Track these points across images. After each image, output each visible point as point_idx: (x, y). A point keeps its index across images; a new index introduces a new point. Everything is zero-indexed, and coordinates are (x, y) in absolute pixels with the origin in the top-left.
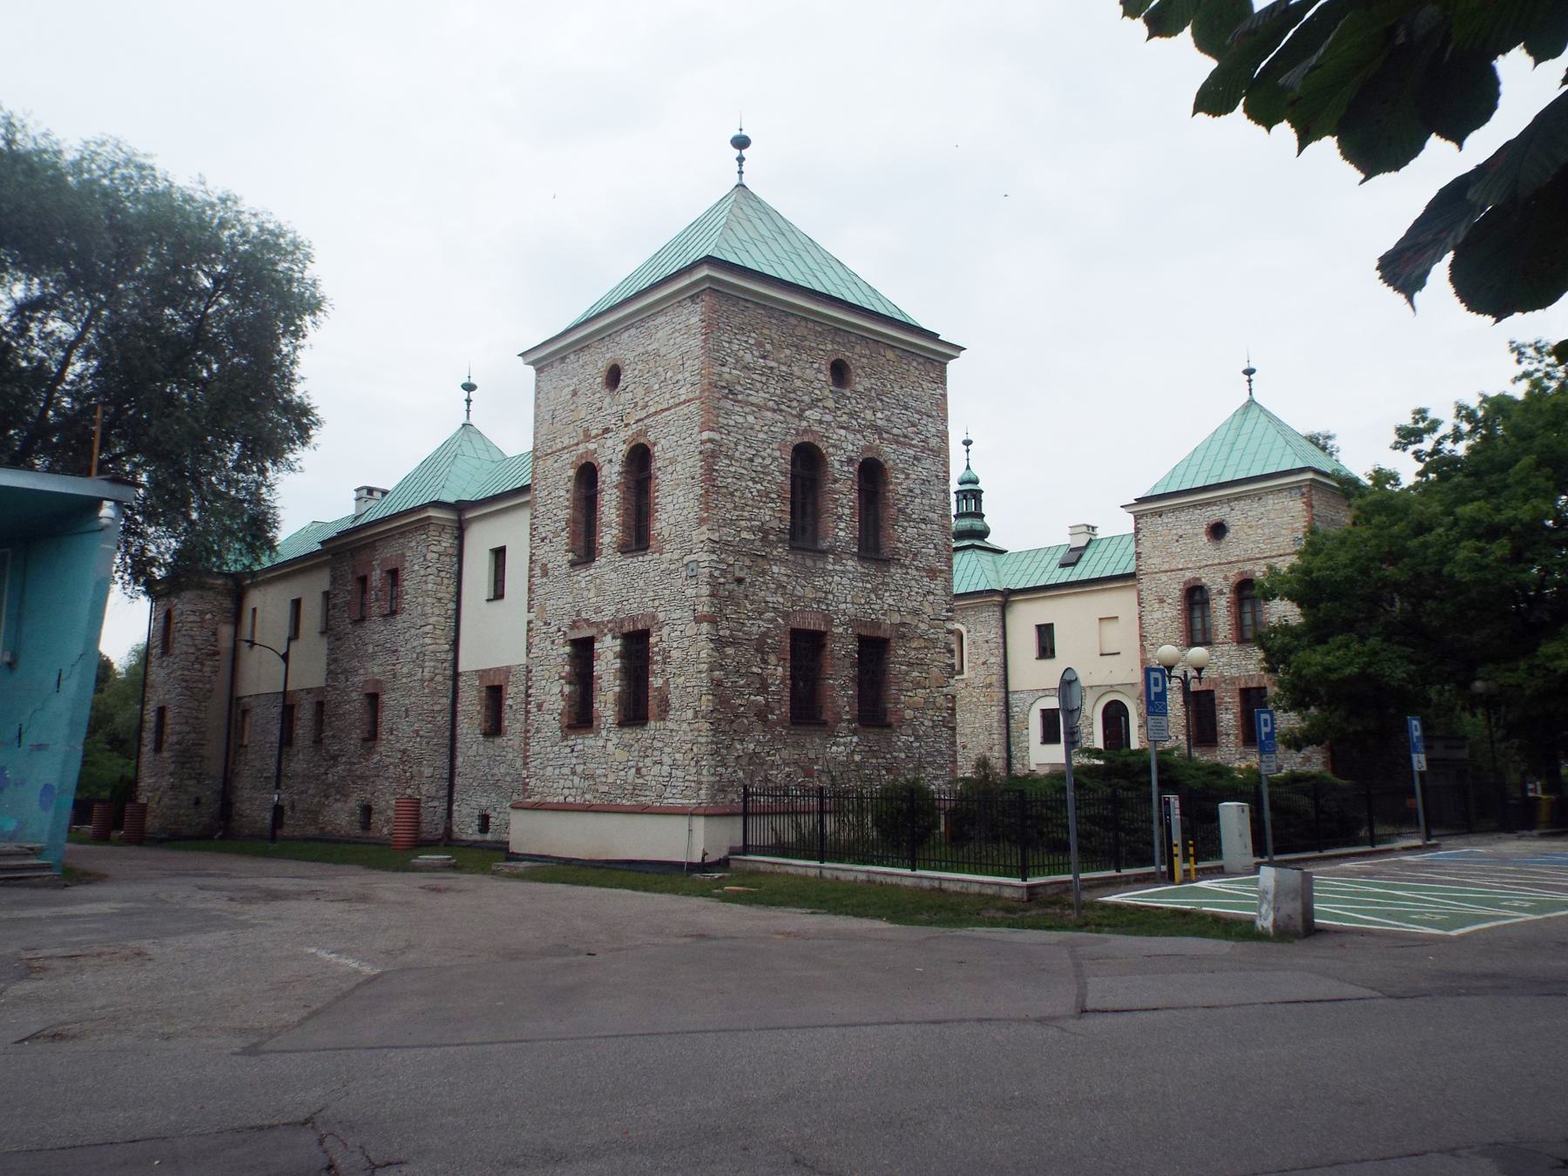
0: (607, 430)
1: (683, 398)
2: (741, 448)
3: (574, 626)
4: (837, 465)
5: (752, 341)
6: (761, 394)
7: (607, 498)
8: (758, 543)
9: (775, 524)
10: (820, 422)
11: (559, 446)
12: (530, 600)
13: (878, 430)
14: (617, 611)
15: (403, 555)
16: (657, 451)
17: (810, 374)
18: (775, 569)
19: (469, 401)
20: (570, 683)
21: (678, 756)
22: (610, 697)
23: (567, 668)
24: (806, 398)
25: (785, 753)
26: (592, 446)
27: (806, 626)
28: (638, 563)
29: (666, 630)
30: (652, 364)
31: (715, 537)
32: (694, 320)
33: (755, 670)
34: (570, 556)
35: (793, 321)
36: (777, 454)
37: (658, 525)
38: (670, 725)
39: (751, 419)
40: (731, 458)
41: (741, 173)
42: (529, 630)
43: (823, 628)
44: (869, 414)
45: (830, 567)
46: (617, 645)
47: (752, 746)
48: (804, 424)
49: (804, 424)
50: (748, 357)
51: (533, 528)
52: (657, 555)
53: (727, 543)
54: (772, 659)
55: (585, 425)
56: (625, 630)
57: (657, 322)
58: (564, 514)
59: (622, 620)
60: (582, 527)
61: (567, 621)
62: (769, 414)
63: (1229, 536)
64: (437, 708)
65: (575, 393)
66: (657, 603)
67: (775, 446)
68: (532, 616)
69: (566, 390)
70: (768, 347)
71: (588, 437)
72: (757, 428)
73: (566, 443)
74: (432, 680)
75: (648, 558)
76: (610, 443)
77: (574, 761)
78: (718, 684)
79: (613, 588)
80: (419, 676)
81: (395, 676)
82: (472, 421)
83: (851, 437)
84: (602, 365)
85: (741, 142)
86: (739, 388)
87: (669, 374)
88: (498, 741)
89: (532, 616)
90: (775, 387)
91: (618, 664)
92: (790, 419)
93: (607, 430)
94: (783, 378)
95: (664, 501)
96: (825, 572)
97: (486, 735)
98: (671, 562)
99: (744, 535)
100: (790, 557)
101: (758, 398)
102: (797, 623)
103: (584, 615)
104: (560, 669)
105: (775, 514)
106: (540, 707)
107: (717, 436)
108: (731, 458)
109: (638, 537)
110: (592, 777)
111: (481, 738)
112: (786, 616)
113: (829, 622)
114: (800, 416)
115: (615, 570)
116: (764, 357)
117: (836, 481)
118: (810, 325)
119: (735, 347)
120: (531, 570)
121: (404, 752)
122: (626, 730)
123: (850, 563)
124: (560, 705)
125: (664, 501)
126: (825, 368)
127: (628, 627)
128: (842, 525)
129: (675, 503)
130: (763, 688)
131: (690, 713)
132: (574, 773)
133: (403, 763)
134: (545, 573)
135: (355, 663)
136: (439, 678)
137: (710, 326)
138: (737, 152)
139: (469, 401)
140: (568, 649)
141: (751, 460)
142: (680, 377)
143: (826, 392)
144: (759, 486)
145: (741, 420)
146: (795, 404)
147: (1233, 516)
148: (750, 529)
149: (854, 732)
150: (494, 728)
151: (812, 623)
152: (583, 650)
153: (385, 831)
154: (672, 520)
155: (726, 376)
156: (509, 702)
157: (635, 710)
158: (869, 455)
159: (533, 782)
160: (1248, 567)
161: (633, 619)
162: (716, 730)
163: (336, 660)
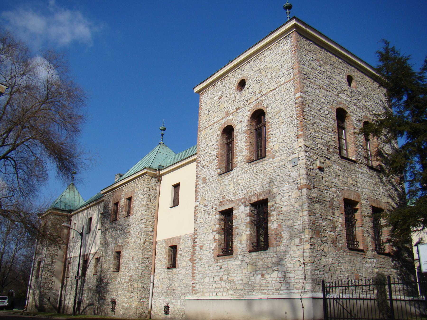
1: (282, 83)
8: (325, 151)
9: (332, 143)
11: (212, 122)
12: (196, 196)
13: (368, 110)
14: (247, 193)
15: (134, 191)
17: (339, 78)
18: (334, 166)
20: (219, 233)
23: (217, 226)
26: (230, 118)
28: (258, 166)
32: (288, 46)
33: (329, 217)
34: (219, 171)
36: (330, 110)
37: (271, 145)
40: (311, 107)
42: (195, 211)
43: (357, 200)
44: (363, 102)
45: (357, 170)
46: (248, 210)
48: (339, 99)
50: (314, 64)
52: (271, 160)
54: (337, 213)
55: (226, 110)
56: (252, 201)
58: (216, 152)
59: (250, 197)
60: (224, 158)
61: (217, 202)
65: (220, 98)
68: (197, 204)
69: (216, 98)
70: (321, 62)
71: (228, 114)
72: (321, 96)
73: (216, 120)
75: (266, 162)
76: (241, 113)
79: (245, 182)
80: (139, 242)
83: (358, 110)
87: (274, 74)
88: (174, 270)
89: (197, 204)
90: (326, 80)
91: (248, 219)
95: (274, 133)
96: (356, 172)
99: (319, 146)
101: (320, 83)
103: (227, 198)
104: (213, 227)
106: (201, 247)
107: (304, 96)
109: (259, 151)
110: (233, 281)
111: (166, 270)
112: (341, 191)
113: (359, 197)
116: (320, 66)
120: (197, 182)
121: (131, 276)
122: (254, 254)
123: (365, 169)
124: (214, 245)
126: (345, 77)
127: (254, 199)
129: (282, 132)
130: (334, 228)
133: (131, 281)
134: (204, 181)
137: (298, 47)
140: (218, 216)
141: (319, 110)
143: (347, 88)
144: (324, 124)
146: (334, 89)
149: (374, 257)
150: (173, 265)
151: (352, 197)
152: (227, 215)
153: (121, 312)
154: (280, 140)
157: (261, 240)
159: (197, 286)
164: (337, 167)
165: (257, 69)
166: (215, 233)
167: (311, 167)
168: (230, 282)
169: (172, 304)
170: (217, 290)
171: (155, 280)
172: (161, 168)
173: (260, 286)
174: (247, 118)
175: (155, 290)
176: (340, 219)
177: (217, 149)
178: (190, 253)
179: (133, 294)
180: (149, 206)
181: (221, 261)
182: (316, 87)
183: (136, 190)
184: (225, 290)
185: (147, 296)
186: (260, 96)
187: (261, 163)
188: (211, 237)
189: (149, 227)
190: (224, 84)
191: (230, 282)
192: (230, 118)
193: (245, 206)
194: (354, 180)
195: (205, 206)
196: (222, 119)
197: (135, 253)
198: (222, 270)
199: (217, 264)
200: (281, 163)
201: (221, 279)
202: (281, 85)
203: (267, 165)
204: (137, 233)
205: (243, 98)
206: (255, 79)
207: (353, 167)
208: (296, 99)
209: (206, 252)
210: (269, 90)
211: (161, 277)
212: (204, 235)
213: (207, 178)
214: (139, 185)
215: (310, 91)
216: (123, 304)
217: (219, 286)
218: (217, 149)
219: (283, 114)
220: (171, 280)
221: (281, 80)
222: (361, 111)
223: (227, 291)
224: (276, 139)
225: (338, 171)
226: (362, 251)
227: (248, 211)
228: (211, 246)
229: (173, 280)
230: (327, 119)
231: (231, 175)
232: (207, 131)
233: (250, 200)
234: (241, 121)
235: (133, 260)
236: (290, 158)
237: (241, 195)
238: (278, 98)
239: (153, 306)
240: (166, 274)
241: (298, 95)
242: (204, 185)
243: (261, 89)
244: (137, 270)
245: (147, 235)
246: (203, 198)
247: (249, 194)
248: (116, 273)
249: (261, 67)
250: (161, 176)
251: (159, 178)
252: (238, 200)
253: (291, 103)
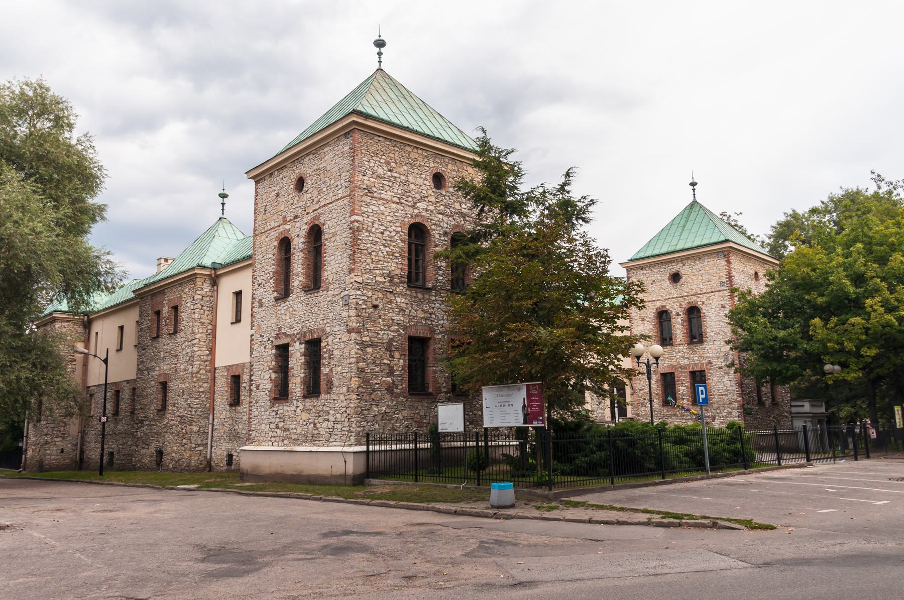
0: (296, 217)
1: (340, 196)
2: (376, 226)
3: (277, 337)
4: (437, 236)
5: (383, 161)
6: (389, 193)
7: (296, 258)
8: (387, 284)
9: (398, 272)
10: (427, 210)
11: (269, 227)
12: (252, 322)
15: (181, 297)
16: (325, 228)
17: (419, 181)
18: (398, 300)
19: (223, 204)
20: (275, 372)
21: (338, 415)
22: (298, 380)
23: (274, 363)
24: (418, 196)
25: (405, 413)
26: (287, 227)
27: (418, 335)
28: (313, 298)
29: (330, 339)
30: (322, 176)
31: (359, 280)
32: (347, 148)
33: (385, 361)
34: (275, 294)
35: (408, 149)
36: (399, 229)
37: (326, 274)
38: (333, 397)
39: (382, 208)
40: (370, 232)
41: (380, 62)
43: (429, 336)
44: (457, 206)
45: (433, 298)
47: (384, 409)
48: (416, 211)
49: (416, 211)
50: (380, 171)
51: (254, 277)
53: (368, 284)
54: (397, 355)
55: (284, 214)
56: (307, 339)
57: (325, 150)
58: (271, 269)
61: (273, 334)
62: (394, 205)
63: (682, 281)
64: (202, 389)
65: (278, 195)
66: (325, 322)
67: (398, 224)
68: (253, 332)
69: (273, 194)
70: (393, 165)
71: (285, 222)
72: (386, 213)
73: (273, 225)
74: (198, 372)
75: (321, 294)
76: (298, 224)
77: (278, 420)
78: (362, 370)
79: (299, 314)
81: (176, 371)
83: (446, 219)
84: (294, 177)
85: (380, 44)
86: (374, 189)
88: (238, 408)
89: (253, 332)
92: (407, 208)
93: (296, 217)
94: (403, 183)
95: (329, 259)
97: (231, 405)
98: (334, 296)
99: (378, 279)
100: (408, 293)
102: (412, 332)
103: (283, 330)
105: (397, 266)
108: (370, 232)
112: (405, 328)
113: (433, 331)
114: (413, 207)
116: (390, 171)
117: (436, 246)
118: (420, 151)
119: (372, 165)
120: (253, 303)
121: (182, 417)
122: (307, 400)
124: (269, 386)
125: (329, 259)
126: (429, 177)
127: (309, 337)
128: (441, 272)
130: (391, 373)
131: (345, 389)
132: (277, 427)
134: (261, 305)
135: (153, 364)
136: (203, 372)
138: (377, 50)
139: (223, 204)
140: (274, 351)
142: (338, 183)
143: (430, 192)
144: (387, 249)
145: (376, 209)
146: (410, 199)
147: (685, 270)
148: (382, 275)
150: (235, 401)
151: (421, 333)
152: (283, 351)
154: (334, 271)
155: (367, 182)
156: (244, 385)
157: (313, 388)
158: (458, 230)
159: (254, 434)
160: (693, 299)
161: (311, 332)
162: (360, 400)
163: (142, 362)
164: (403, 300)
165: (315, 167)
167: (364, 307)
168: (286, 430)
170: (273, 439)
171: (216, 420)
172: (217, 266)
175: (215, 434)
176: (402, 361)
179: (184, 441)
180: (203, 321)
182: (380, 202)
183: (184, 296)
185: (204, 442)
191: (286, 430)
194: (425, 312)
201: (277, 427)
203: (322, 298)
205: (301, 204)
207: (427, 296)
213: (263, 301)
214: (187, 290)
215: (370, 210)
216: (173, 455)
217: (275, 434)
220: (235, 421)
222: (451, 219)
223: (283, 440)
225: (405, 305)
226: (431, 394)
227: (303, 350)
230: (393, 242)
232: (264, 237)
234: (298, 236)
236: (343, 294)
237: (297, 328)
239: (213, 455)
245: (202, 361)
246: (259, 327)
247: (304, 330)
248: (162, 413)
249: (321, 166)
250: (218, 277)
251: (215, 281)
253: (346, 226)
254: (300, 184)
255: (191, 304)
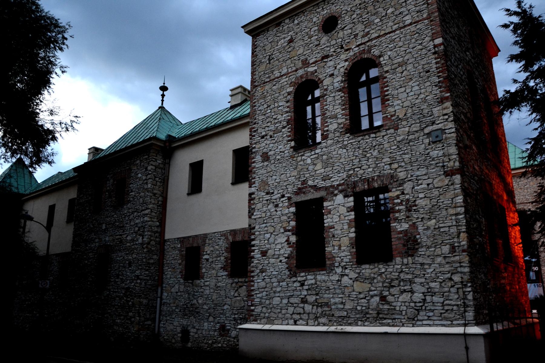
1: (407, 22)
3: (299, 192)
14: (349, 176)
21: (433, 285)
22: (345, 241)
23: (293, 223)
26: (311, 69)
29: (408, 187)
38: (421, 260)
42: (250, 201)
52: (392, 131)
55: (302, 58)
58: (284, 117)
59: (355, 184)
64: (152, 261)
65: (291, 41)
66: (395, 166)
71: (306, 64)
73: (285, 71)
74: (148, 243)
77: (305, 293)
80: (140, 241)
81: (121, 242)
82: (164, 105)
89: (253, 190)
106: (264, 253)
110: (327, 304)
115: (345, 147)
131: (446, 249)
132: (304, 301)
135: (93, 236)
136: (153, 243)
156: (206, 257)
166: (290, 233)
169: (194, 328)
170: (296, 317)
173: (378, 314)
174: (342, 70)
177: (287, 112)
178: (222, 258)
180: (155, 191)
181: (303, 274)
184: (312, 316)
185: (152, 316)
186: (366, 39)
187: (373, 135)
188: (282, 239)
189: (155, 220)
190: (296, 22)
192: (311, 69)
193: (345, 196)
195: (267, 193)
196: (296, 70)
197: (134, 256)
198: (306, 287)
199: (294, 279)
200: (411, 137)
202: (405, 26)
204: (137, 229)
205: (333, 42)
206: (355, 16)
208: (435, 46)
209: (272, 261)
210: (383, 32)
211: (173, 290)
212: (268, 236)
214: (138, 162)
218: (287, 112)
219: (410, 67)
221: (405, 19)
223: (316, 318)
224: (399, 102)
228: (282, 252)
229: (194, 295)
231: (317, 151)
233: (355, 187)
235: (130, 265)
237: (337, 179)
238: (401, 44)
239: (162, 330)
240: (182, 287)
241: (439, 41)
242: (266, 163)
243: (367, 30)
244: (139, 281)
245: (152, 231)
252: (332, 186)
254: (330, 25)
255: (141, 178)
